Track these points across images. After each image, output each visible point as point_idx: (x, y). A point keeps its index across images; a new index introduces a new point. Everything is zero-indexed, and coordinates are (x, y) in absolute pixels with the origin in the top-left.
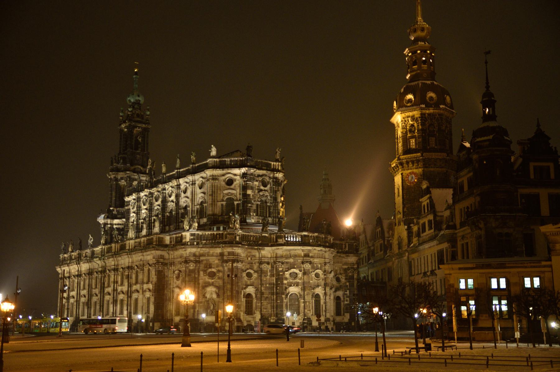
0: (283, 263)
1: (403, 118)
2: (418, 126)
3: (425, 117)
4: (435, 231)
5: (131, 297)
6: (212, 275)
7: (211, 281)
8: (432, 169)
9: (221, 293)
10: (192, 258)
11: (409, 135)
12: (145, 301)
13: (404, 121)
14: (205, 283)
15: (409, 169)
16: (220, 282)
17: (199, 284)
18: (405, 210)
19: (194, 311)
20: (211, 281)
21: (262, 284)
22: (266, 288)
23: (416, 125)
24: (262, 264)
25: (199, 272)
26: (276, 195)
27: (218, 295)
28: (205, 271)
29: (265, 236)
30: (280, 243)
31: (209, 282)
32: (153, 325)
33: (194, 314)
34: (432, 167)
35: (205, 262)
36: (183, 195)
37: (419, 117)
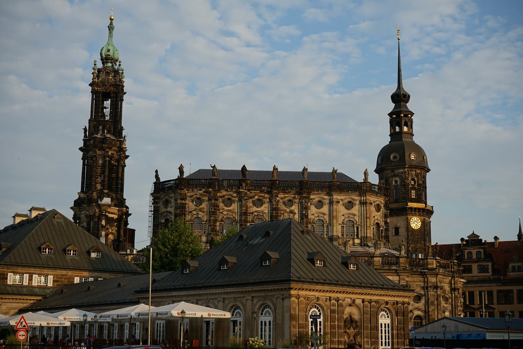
4: (493, 275)
14: (444, 307)
18: (410, 249)
36: (313, 210)
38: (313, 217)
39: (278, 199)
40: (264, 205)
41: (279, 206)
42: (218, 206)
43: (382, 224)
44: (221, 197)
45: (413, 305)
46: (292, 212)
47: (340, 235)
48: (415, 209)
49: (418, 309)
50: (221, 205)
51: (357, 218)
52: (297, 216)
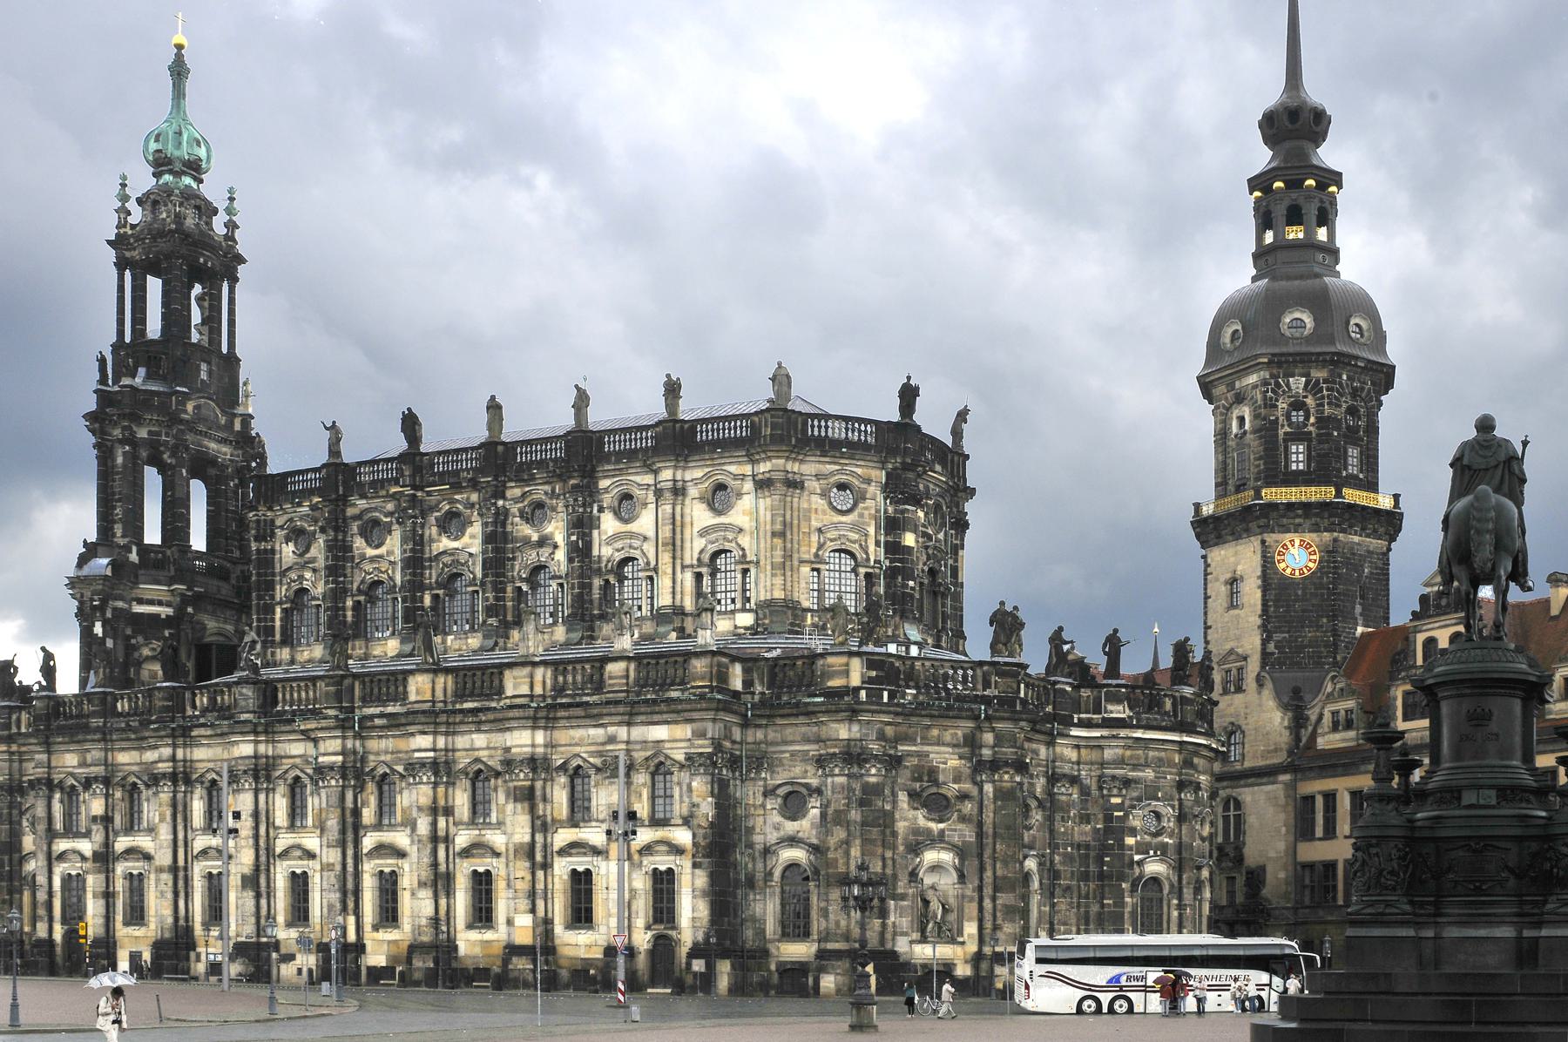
0: (1127, 783)
5: (547, 866)
6: (937, 805)
7: (935, 827)
8: (1356, 539)
9: (971, 866)
10: (874, 747)
12: (641, 883)
14: (917, 831)
16: (968, 834)
17: (894, 834)
19: (884, 925)
20: (935, 827)
21: (1054, 847)
22: (1068, 858)
24: (1058, 780)
25: (894, 795)
26: (956, 561)
27: (962, 877)
28: (913, 795)
31: (929, 831)
32: (710, 967)
33: (882, 934)
35: (911, 762)
38: (607, 552)
39: (500, 503)
40: (469, 530)
41: (509, 528)
42: (350, 549)
43: (876, 553)
44: (355, 518)
45: (777, 827)
46: (543, 542)
47: (689, 604)
48: (1290, 506)
49: (793, 841)
50: (359, 543)
51: (745, 541)
52: (561, 555)
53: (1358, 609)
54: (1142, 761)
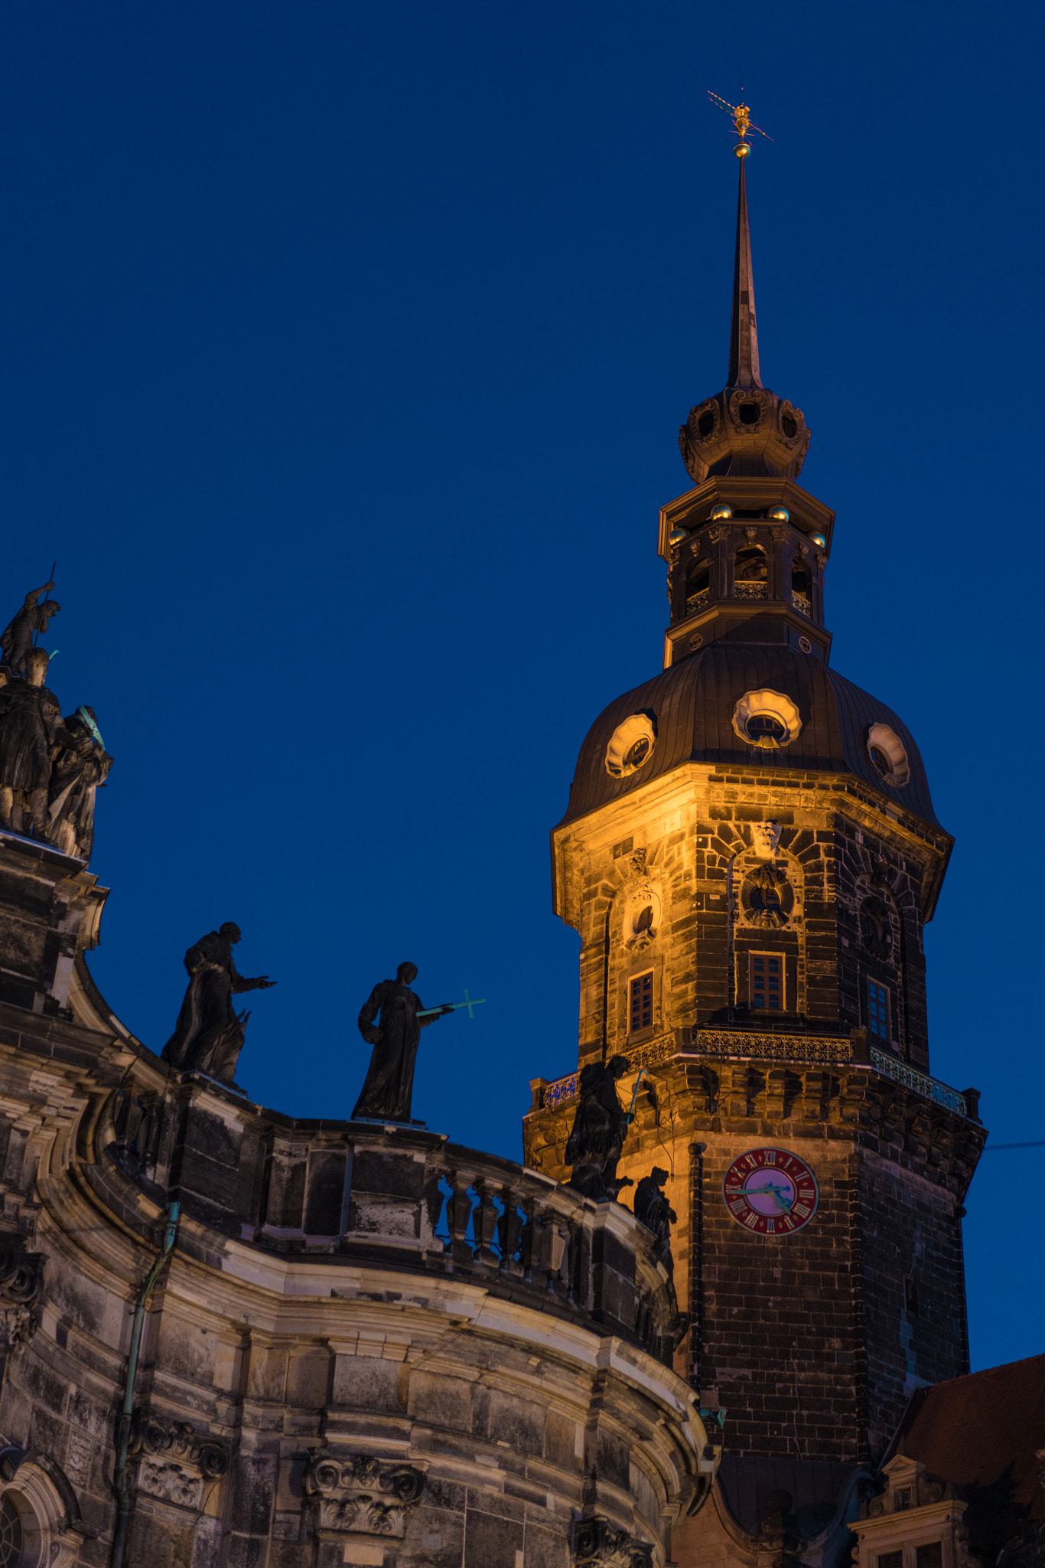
0: (410, 1484)
1: (714, 814)
2: (815, 881)
3: (852, 849)
8: (896, 1170)
11: (743, 923)
13: (717, 836)
15: (751, 1130)
23: (795, 873)
24: (155, 1438)
29: (218, 1125)
30: (382, 1239)
34: (894, 1157)
37: (823, 836)
53: (906, 1333)
54: (467, 1422)
